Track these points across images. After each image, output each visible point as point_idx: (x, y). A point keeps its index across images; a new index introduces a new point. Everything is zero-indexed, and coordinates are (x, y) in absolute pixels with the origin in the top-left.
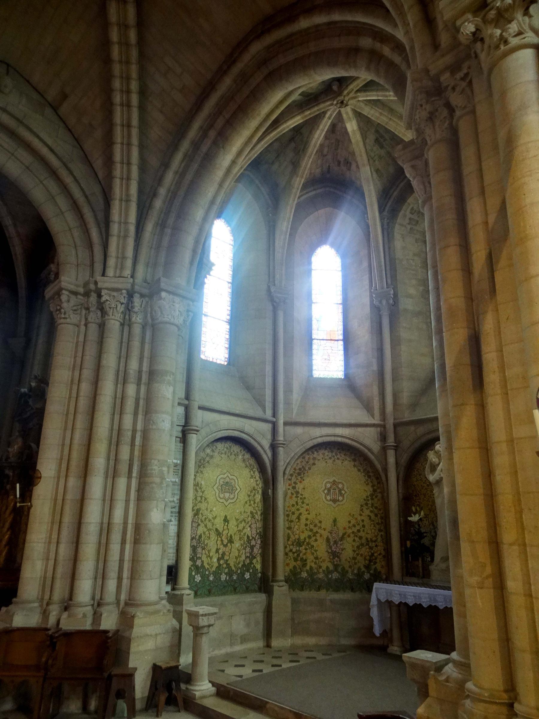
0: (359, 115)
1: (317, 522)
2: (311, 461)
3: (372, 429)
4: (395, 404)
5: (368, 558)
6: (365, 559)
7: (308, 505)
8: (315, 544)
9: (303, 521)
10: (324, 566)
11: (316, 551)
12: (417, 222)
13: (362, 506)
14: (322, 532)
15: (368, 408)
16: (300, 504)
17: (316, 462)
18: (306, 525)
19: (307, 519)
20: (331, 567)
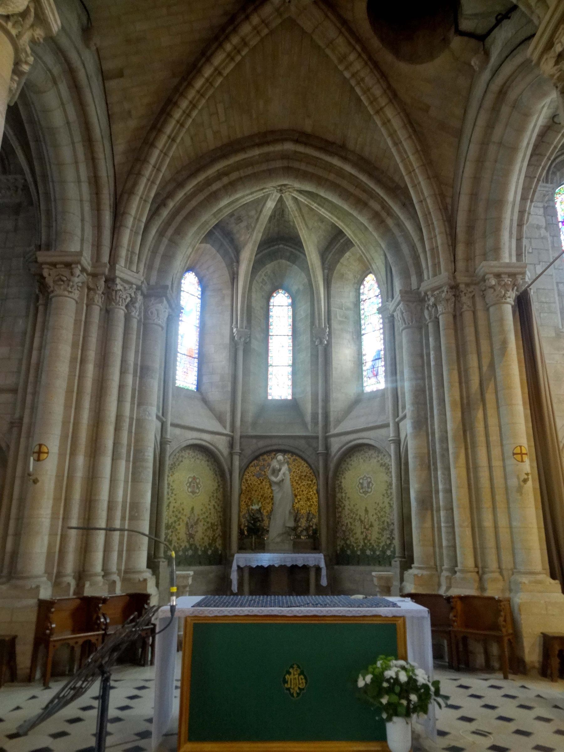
0: (281, 200)
1: (181, 509)
2: (180, 459)
3: (224, 438)
5: (211, 538)
6: (209, 539)
7: (175, 495)
8: (177, 527)
9: (171, 509)
10: (183, 545)
11: (179, 533)
12: (266, 283)
13: (210, 498)
14: (183, 517)
15: (220, 419)
16: (170, 494)
17: (183, 459)
18: (173, 512)
19: (174, 507)
20: (188, 546)
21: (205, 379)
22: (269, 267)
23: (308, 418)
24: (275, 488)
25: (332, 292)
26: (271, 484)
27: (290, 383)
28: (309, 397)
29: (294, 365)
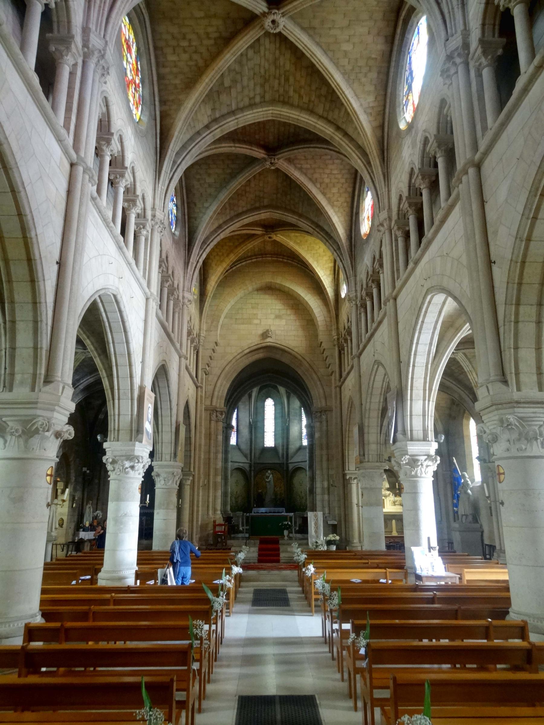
15: (246, 456)
21: (239, 440)
22: (264, 391)
23: (280, 455)
24: (268, 484)
25: (290, 403)
26: (266, 482)
27: (273, 439)
29: (275, 432)
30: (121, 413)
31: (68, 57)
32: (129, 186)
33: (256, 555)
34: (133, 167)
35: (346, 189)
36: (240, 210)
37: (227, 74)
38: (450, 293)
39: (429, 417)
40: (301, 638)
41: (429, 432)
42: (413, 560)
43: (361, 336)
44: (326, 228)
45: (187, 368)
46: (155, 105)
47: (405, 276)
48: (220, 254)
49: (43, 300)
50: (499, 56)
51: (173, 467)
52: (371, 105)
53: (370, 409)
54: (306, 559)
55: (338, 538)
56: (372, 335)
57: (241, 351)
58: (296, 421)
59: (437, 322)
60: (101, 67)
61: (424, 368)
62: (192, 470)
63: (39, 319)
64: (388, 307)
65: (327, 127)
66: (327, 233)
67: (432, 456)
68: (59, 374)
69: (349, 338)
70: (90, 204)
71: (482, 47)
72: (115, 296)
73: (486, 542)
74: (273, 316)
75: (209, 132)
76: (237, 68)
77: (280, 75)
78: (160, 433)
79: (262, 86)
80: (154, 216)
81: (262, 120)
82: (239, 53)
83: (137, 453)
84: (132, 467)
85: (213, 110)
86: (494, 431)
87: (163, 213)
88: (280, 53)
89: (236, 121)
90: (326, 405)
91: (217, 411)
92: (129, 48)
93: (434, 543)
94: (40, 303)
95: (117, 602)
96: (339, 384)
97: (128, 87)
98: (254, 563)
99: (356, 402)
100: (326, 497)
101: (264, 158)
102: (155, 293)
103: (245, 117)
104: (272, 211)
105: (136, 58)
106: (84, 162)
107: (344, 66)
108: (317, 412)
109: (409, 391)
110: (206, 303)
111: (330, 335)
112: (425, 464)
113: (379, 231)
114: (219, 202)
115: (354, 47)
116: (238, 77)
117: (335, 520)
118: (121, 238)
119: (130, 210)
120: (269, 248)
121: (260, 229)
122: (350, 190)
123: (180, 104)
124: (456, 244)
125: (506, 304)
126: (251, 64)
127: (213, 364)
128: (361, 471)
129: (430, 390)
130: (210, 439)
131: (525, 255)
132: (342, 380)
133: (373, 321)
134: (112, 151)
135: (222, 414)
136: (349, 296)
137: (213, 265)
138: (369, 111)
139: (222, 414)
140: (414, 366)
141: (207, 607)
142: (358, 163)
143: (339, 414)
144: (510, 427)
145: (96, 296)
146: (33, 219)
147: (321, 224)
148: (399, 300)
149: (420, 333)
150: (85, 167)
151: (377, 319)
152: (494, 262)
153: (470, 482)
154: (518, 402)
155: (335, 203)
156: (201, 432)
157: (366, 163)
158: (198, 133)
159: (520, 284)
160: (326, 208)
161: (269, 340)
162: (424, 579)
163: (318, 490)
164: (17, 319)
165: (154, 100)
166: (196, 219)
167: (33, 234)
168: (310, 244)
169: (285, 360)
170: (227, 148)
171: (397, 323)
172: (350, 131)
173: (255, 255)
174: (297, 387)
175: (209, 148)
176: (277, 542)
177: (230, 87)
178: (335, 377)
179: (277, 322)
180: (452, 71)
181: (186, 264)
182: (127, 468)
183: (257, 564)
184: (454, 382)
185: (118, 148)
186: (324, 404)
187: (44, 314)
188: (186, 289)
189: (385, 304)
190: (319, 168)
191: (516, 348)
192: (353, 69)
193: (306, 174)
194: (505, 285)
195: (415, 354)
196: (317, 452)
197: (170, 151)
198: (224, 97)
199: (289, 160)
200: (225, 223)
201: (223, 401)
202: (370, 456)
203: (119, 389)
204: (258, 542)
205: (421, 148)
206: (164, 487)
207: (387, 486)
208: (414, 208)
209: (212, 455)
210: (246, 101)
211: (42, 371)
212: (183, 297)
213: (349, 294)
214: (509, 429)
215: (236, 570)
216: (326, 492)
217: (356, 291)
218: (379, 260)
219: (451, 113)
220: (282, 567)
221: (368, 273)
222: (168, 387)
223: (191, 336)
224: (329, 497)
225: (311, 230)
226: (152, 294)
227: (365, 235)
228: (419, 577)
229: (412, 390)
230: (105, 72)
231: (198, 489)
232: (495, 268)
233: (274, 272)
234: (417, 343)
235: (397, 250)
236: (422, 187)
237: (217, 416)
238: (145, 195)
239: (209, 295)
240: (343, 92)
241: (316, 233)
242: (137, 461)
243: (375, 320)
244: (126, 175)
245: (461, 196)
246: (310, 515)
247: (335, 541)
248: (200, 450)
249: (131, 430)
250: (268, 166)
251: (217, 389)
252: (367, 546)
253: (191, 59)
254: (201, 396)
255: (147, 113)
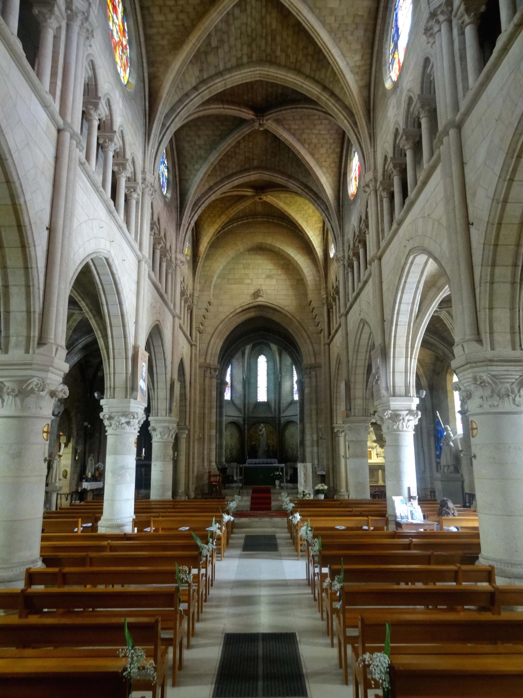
4: (248, 411)
15: (239, 411)
21: (234, 395)
22: (257, 348)
23: (273, 410)
26: (259, 435)
27: (266, 394)
28: (273, 402)
29: (268, 387)
30: (117, 371)
31: (52, 20)
32: (118, 150)
33: (248, 503)
34: (122, 131)
35: (334, 149)
36: (230, 172)
37: (214, 33)
38: (431, 255)
39: (411, 374)
40: (287, 580)
41: (411, 388)
42: (394, 509)
43: (348, 295)
44: (315, 189)
45: (181, 327)
46: (143, 67)
47: (389, 237)
48: (212, 215)
49: (34, 265)
50: (482, 14)
51: (169, 422)
52: (358, 64)
53: (356, 366)
54: (293, 507)
55: (326, 487)
56: (358, 294)
57: (233, 310)
58: (288, 378)
59: (419, 282)
60: (85, 30)
61: (407, 327)
62: (187, 424)
63: (31, 284)
64: (372, 267)
65: (314, 87)
66: (315, 194)
67: (413, 411)
68: (52, 337)
69: (337, 297)
70: (79, 169)
71: (464, 4)
72: (107, 259)
73: (467, 490)
74: (264, 276)
75: (197, 93)
76: (224, 27)
77: (267, 35)
78: (156, 390)
79: (250, 45)
80: (144, 179)
81: (250, 80)
82: (225, 12)
83: (132, 410)
84: (128, 423)
85: (201, 71)
86: (468, 388)
87: (153, 177)
88: (267, 11)
89: (224, 82)
90: (316, 362)
91: (211, 368)
92: (115, 8)
93: (414, 493)
94: (31, 268)
95: (112, 548)
96: (327, 341)
97: (115, 48)
98: (247, 511)
99: (344, 359)
100: (315, 449)
101: (253, 119)
102: (147, 256)
103: (233, 78)
104: (262, 172)
105: (123, 18)
106: (72, 128)
107: (330, 24)
108: (306, 368)
109: (392, 349)
110: (199, 264)
111: (320, 293)
112: (407, 418)
113: (365, 192)
114: (209, 164)
115: (340, 4)
116: (225, 37)
117: (324, 471)
118: (112, 203)
119: (120, 174)
120: (259, 208)
121: (251, 190)
122: (338, 150)
123: (167, 66)
124: (437, 205)
125: (482, 265)
126: (237, 23)
127: (207, 323)
128: (348, 425)
129: (413, 347)
130: (204, 395)
131: (501, 218)
132: (331, 337)
133: (359, 280)
134: (99, 115)
135: (215, 371)
136: (336, 256)
137: (205, 226)
138: (356, 70)
139: (215, 371)
140: (397, 325)
141: (196, 553)
142: (345, 124)
143: (328, 371)
144: (483, 384)
145: (89, 260)
146: (21, 186)
147: (310, 184)
148: (383, 260)
149: (403, 292)
150: (72, 132)
151: (363, 278)
152: (472, 224)
153: (452, 435)
154: (491, 361)
155: (324, 163)
156: (195, 389)
157: (352, 124)
158: (187, 95)
159: (496, 245)
160: (314, 169)
161: (260, 299)
162: (403, 527)
163: (308, 443)
164: (10, 284)
165: (142, 63)
166: (187, 181)
167: (22, 201)
168: (300, 204)
169: (276, 318)
170: (215, 109)
171: (381, 283)
172: (337, 91)
173: (246, 216)
174: (288, 345)
175: (198, 110)
176: (268, 491)
177: (217, 48)
178: (324, 335)
179: (268, 282)
180: (436, 29)
181: (179, 225)
182: (123, 424)
183: (249, 512)
184: (438, 339)
185: (105, 112)
186: (313, 361)
187: (36, 279)
188: (178, 251)
189: (370, 264)
190: (307, 128)
191: (491, 308)
192: (339, 27)
193: (294, 135)
194: (482, 246)
195: (398, 314)
196: (307, 407)
197: (158, 113)
198: (211, 58)
199: (278, 121)
200: (216, 184)
201: (216, 359)
202: (357, 411)
203: (113, 349)
204: (251, 491)
205: (406, 108)
206: (160, 440)
207: (374, 438)
208: (398, 169)
209: (206, 411)
210: (234, 62)
211: (35, 333)
212: (176, 259)
213: (337, 254)
214: (482, 387)
215: (227, 518)
216: (316, 445)
217: (344, 251)
218: (364, 221)
219: (433, 72)
220: (273, 514)
221: (355, 233)
222: (163, 345)
223: (185, 297)
224: (318, 449)
225: (299, 191)
226: (144, 256)
227: (352, 195)
228: (399, 525)
229: (394, 347)
230: (90, 34)
231: (194, 442)
232: (473, 230)
233: (264, 233)
234: (400, 303)
235: (382, 211)
236: (406, 148)
237: (211, 373)
238: (135, 158)
239: (201, 256)
240: (330, 51)
241: (304, 193)
242: (132, 417)
243: (361, 280)
244: (115, 139)
245: (442, 158)
246: (300, 466)
247: (323, 490)
248: (195, 406)
249: (126, 388)
250: (256, 128)
251: (210, 348)
252: (353, 496)
253: (177, 19)
254: (196, 354)
255: (135, 76)
